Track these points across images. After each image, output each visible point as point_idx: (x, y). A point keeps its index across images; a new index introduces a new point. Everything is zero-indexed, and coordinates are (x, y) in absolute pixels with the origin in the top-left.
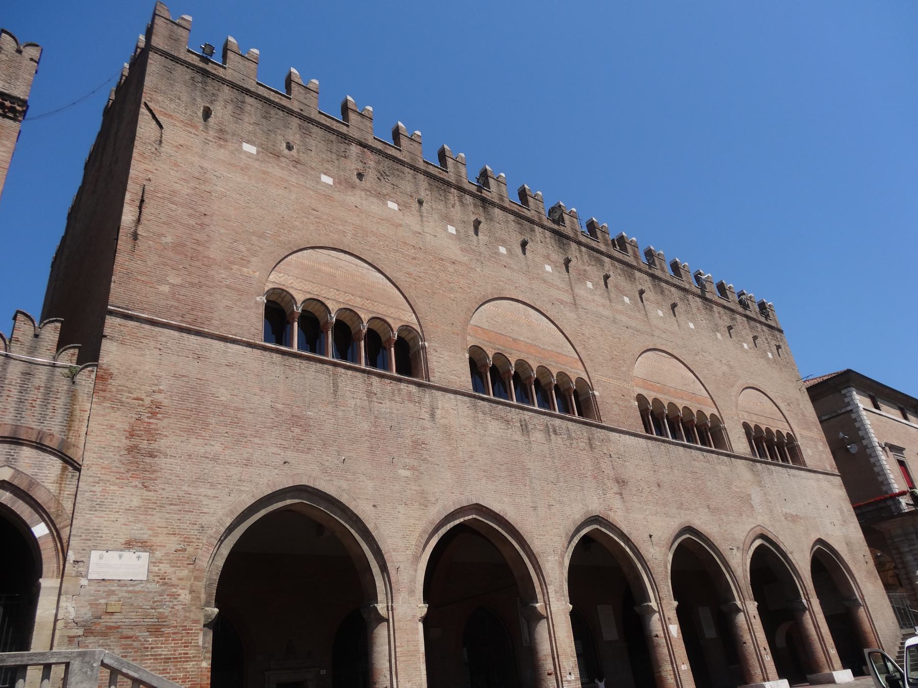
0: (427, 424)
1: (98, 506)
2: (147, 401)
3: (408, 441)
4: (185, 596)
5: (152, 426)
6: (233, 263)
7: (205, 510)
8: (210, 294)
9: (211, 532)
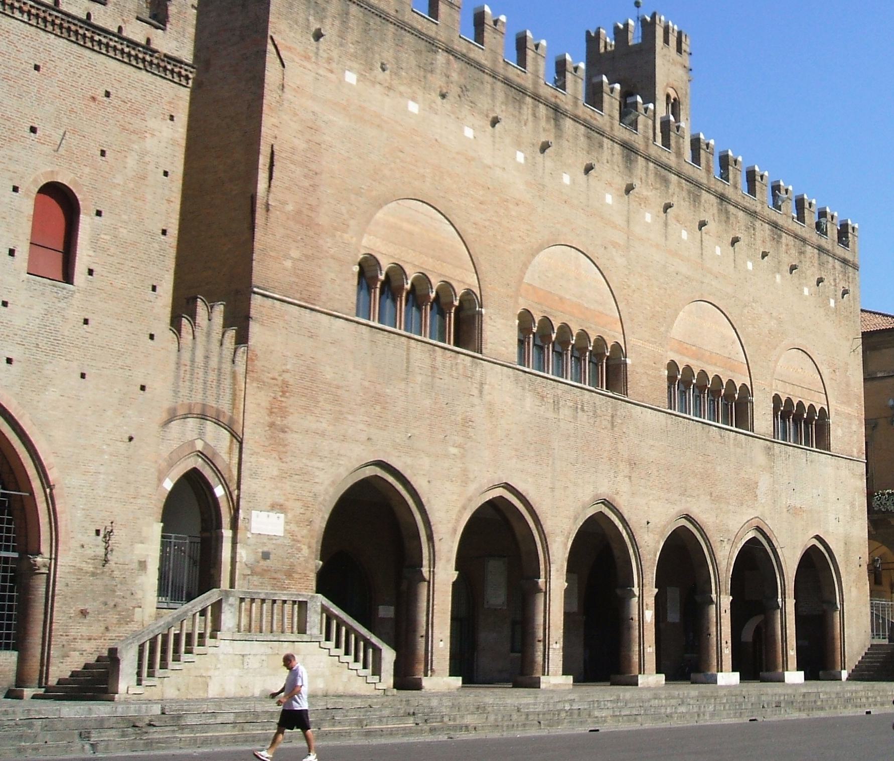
0: (476, 401)
1: (254, 475)
2: (279, 383)
3: (459, 419)
4: (305, 551)
5: (284, 404)
6: (336, 229)
7: (317, 480)
8: (320, 267)
9: (321, 499)
